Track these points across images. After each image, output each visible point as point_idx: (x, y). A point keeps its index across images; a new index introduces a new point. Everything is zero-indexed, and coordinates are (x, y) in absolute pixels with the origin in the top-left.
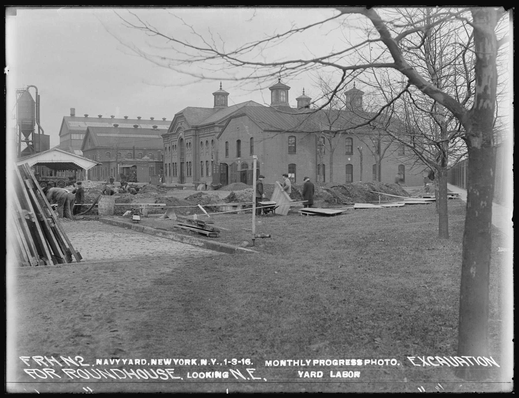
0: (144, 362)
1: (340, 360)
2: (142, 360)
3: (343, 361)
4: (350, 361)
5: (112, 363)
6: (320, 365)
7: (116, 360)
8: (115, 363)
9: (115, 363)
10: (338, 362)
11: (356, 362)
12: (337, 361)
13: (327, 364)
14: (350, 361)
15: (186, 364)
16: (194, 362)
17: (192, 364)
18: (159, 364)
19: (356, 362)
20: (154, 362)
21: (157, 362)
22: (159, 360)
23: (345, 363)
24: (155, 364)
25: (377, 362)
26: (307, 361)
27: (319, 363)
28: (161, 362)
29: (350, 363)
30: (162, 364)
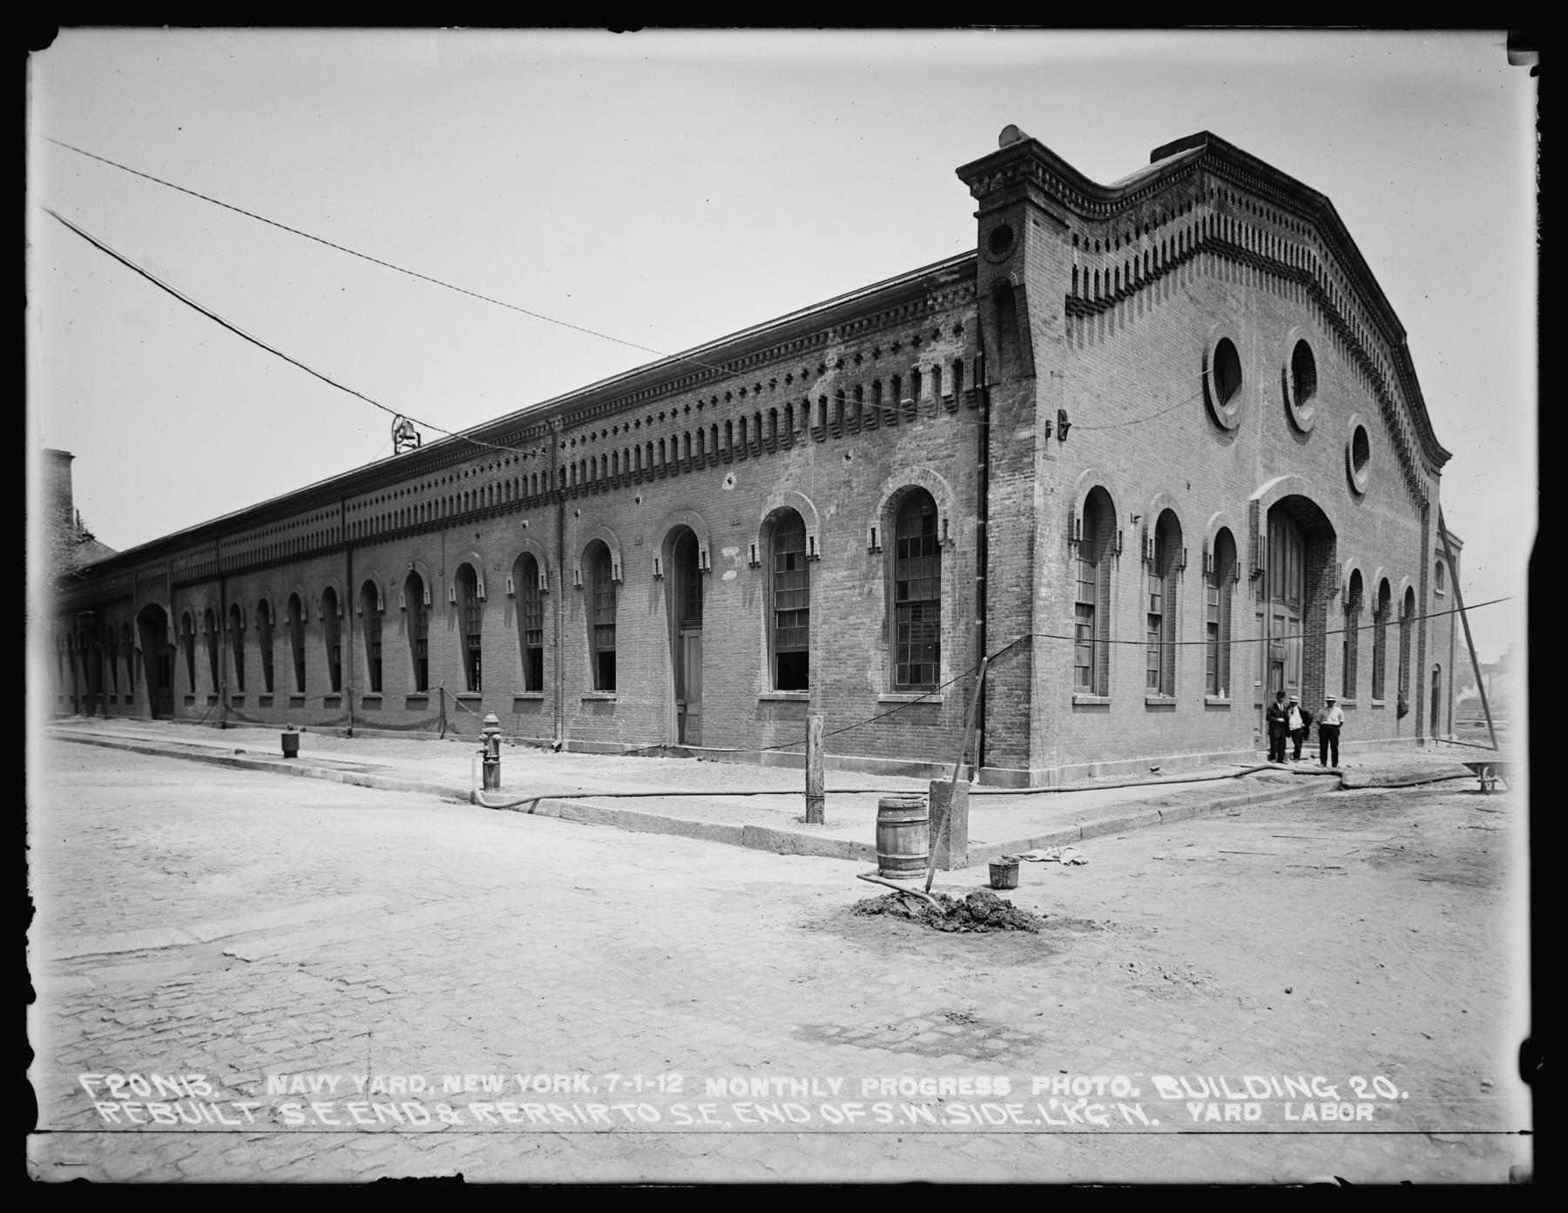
0: (418, 1084)
1: (943, 1081)
2: (413, 1078)
3: (953, 1081)
4: (973, 1084)
5: (316, 1088)
6: (884, 1092)
7: (328, 1078)
8: (325, 1084)
9: (325, 1084)
10: (937, 1085)
11: (991, 1083)
12: (933, 1081)
13: (904, 1092)
14: (973, 1084)
15: (556, 1090)
16: (581, 1082)
17: (576, 1089)
18: (467, 1088)
19: (991, 1083)
20: (451, 1084)
21: (462, 1082)
22: (467, 1078)
23: (957, 1087)
24: (456, 1089)
25: (1071, 1084)
26: (830, 1080)
27: (879, 1090)
28: (474, 1083)
29: (974, 1087)
30: (477, 1089)
